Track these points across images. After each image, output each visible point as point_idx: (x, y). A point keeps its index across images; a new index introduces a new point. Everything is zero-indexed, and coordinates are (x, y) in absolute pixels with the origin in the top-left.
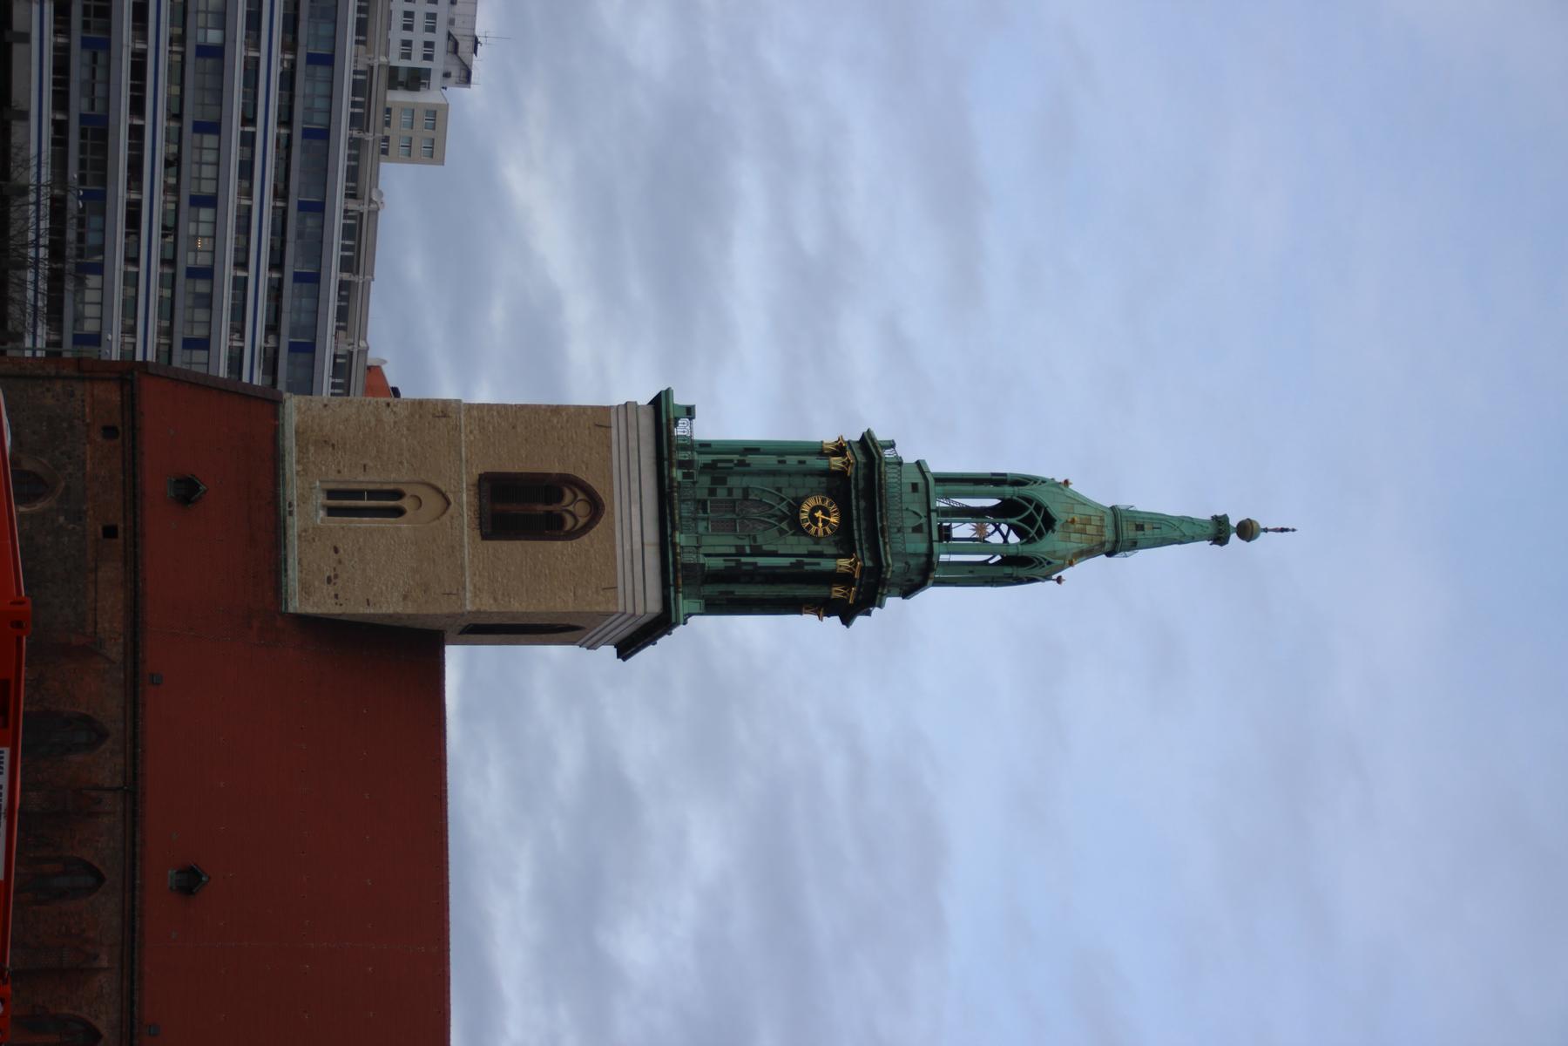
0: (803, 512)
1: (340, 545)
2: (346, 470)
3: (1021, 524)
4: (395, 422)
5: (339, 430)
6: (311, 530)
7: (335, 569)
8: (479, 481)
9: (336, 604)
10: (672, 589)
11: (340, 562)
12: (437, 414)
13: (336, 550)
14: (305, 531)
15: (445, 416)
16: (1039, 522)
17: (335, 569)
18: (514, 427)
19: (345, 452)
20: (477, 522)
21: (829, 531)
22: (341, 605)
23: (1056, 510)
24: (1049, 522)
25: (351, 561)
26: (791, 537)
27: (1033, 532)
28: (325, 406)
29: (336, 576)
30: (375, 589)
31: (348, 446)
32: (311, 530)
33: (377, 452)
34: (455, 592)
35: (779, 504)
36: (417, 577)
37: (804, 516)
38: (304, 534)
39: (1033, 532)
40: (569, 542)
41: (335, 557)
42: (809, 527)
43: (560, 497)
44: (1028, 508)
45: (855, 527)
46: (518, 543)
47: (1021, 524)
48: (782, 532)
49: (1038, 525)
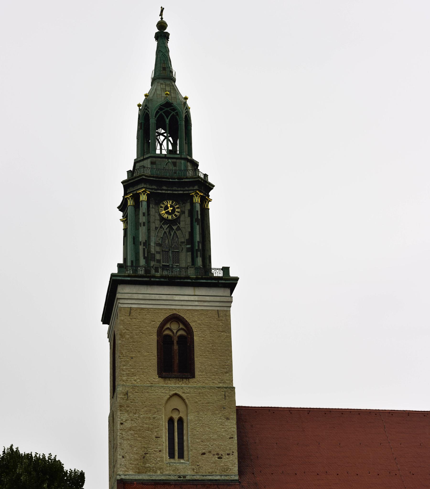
0: (168, 217)
1: (201, 452)
2: (158, 447)
3: (169, 118)
4: (132, 420)
5: (136, 450)
6: (193, 467)
7: (214, 455)
8: (162, 378)
9: (232, 455)
10: (220, 281)
11: (210, 452)
12: (127, 398)
13: (204, 454)
14: (193, 470)
15: (127, 394)
16: (168, 109)
17: (214, 455)
18: (132, 358)
19: (149, 448)
20: (185, 380)
21: (177, 206)
22: (233, 452)
23: (160, 101)
24: (168, 104)
25: (209, 446)
26: (181, 224)
27: (173, 113)
28: (123, 457)
29: (218, 454)
30: (224, 434)
31: (146, 446)
32: (193, 467)
33: (148, 430)
34: (224, 393)
35: (164, 229)
36: (217, 412)
37: (170, 217)
38: (195, 471)
39: (173, 113)
40: (194, 333)
41: (207, 454)
42: (175, 215)
43: (167, 336)
44: (161, 114)
45: (177, 192)
46: (196, 359)
47: (169, 118)
48: (179, 229)
49: (169, 110)
